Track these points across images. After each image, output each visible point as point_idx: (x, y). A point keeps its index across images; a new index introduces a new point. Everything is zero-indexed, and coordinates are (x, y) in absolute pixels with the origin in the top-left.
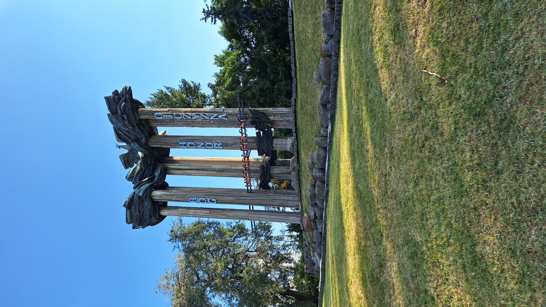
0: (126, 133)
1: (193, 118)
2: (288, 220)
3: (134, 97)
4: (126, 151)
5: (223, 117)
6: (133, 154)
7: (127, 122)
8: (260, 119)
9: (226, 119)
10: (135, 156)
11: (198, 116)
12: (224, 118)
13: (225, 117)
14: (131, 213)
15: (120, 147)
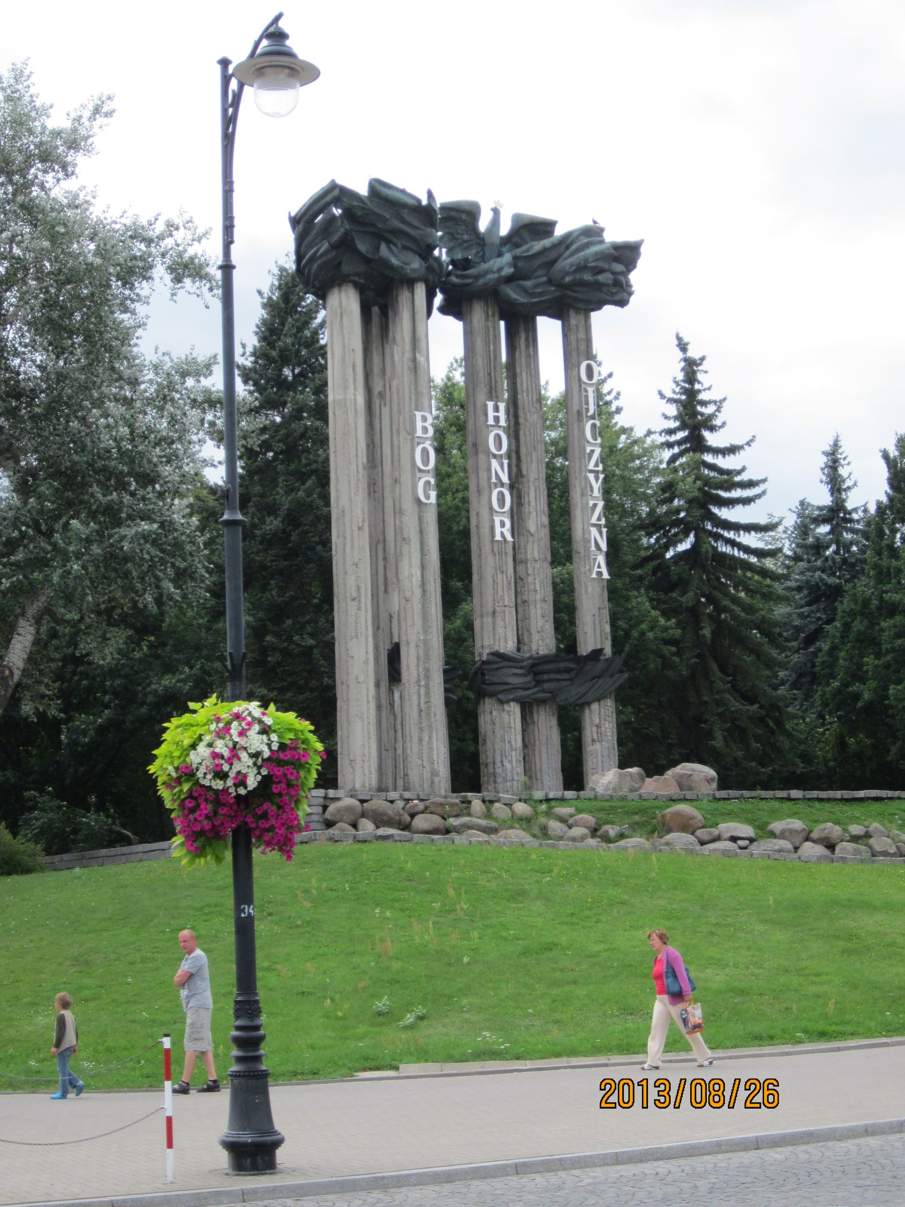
0: (552, 256)
1: (591, 476)
2: (369, 738)
3: (608, 309)
4: (483, 225)
5: (599, 567)
6: (466, 241)
7: (587, 277)
8: (599, 677)
9: (594, 576)
10: (460, 245)
11: (597, 493)
12: (596, 569)
13: (600, 574)
14: (404, 206)
15: (496, 211)
